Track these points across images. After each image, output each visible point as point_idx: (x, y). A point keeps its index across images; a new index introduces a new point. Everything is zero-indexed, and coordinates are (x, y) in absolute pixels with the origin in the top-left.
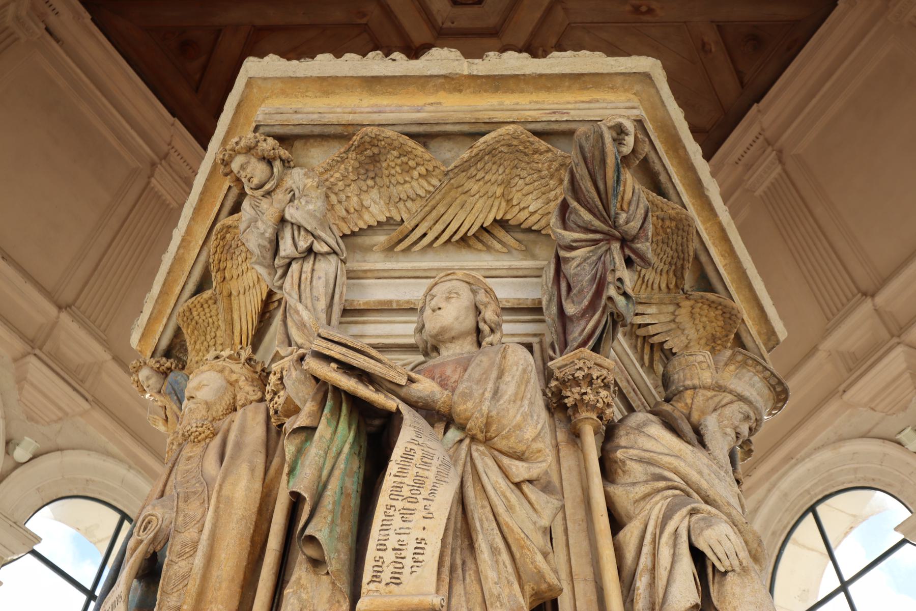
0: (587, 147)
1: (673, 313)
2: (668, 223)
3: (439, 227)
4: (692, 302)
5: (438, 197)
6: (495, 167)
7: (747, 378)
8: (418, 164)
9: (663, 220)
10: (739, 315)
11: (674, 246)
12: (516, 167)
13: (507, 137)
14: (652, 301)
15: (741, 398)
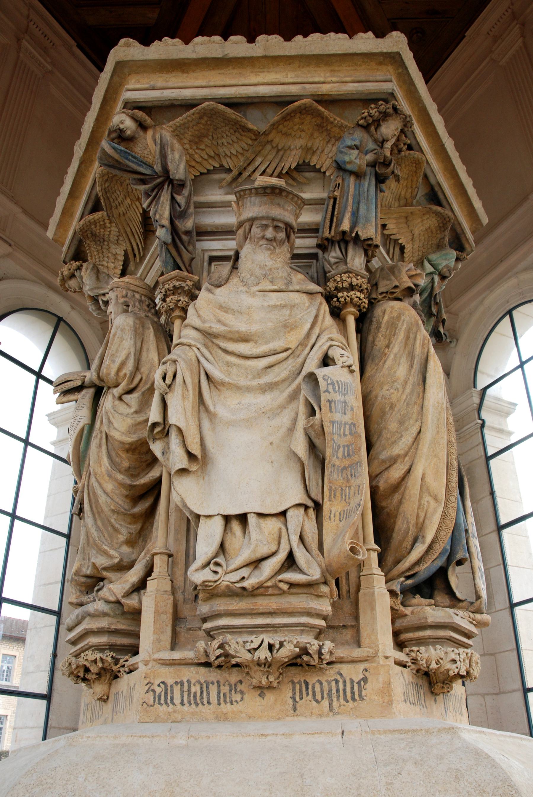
0: (105, 162)
1: (273, 148)
2: (203, 121)
3: (136, 236)
4: (274, 132)
5: (120, 227)
6: (115, 194)
7: (249, 204)
8: (104, 221)
9: (198, 123)
10: (307, 105)
11: (223, 125)
12: (121, 184)
13: (101, 180)
14: (251, 159)
15: (252, 220)
